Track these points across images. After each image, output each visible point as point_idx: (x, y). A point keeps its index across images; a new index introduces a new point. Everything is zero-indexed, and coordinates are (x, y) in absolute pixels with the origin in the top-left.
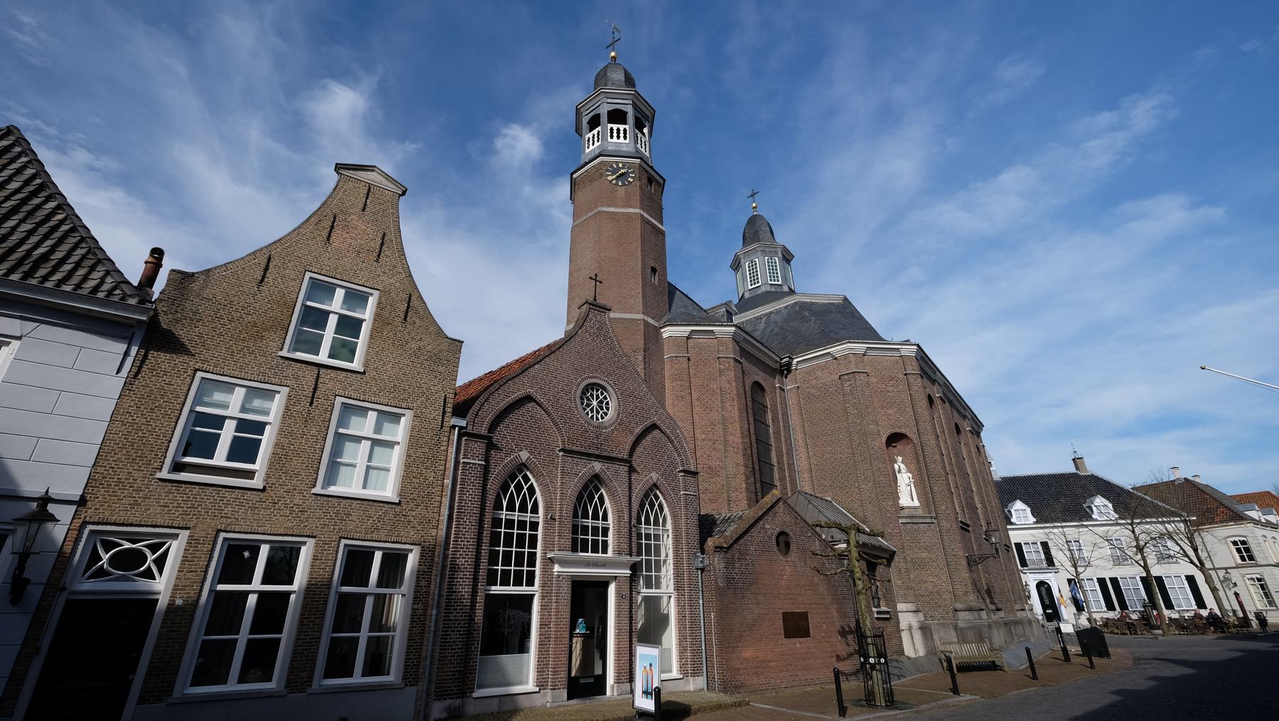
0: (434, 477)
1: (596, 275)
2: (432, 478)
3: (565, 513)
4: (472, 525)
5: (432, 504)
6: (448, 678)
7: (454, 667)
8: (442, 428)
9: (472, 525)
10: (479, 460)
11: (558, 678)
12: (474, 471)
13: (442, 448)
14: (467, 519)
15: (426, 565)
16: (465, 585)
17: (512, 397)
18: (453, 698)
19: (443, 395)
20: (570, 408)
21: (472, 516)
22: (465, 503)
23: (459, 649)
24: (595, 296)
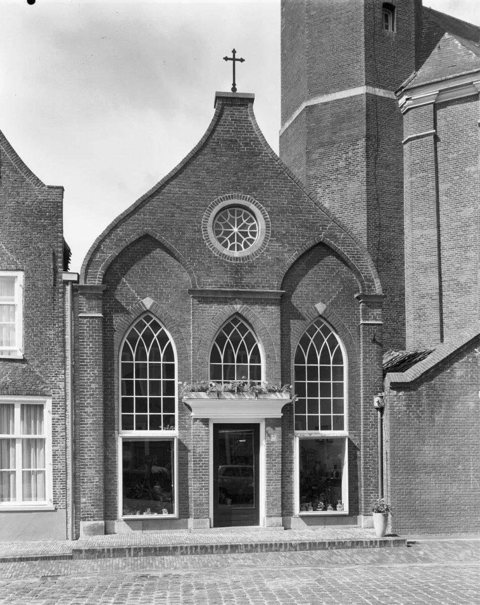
1: (234, 52)
24: (234, 84)
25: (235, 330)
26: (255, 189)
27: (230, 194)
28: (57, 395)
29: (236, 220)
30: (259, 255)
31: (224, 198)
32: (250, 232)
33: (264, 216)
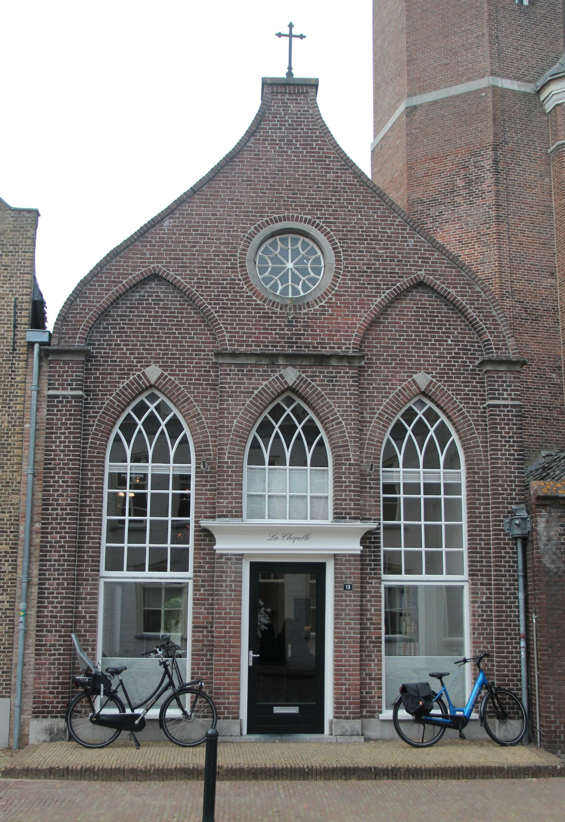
0: (9, 422)
2: (6, 424)
3: (228, 458)
4: (67, 486)
5: (10, 460)
6: (47, 691)
7: (54, 678)
8: (14, 350)
9: (67, 486)
10: (72, 389)
11: (224, 703)
12: (66, 406)
13: (18, 379)
14: (59, 477)
15: (8, 544)
16: (63, 570)
17: (124, 281)
18: (57, 717)
19: (13, 300)
20: (233, 283)
21: (68, 473)
22: (55, 455)
23: (59, 654)
25: (288, 415)
26: (319, 207)
27: (281, 215)
28: (8, 515)
29: (290, 251)
30: (324, 301)
31: (271, 220)
32: (312, 269)
33: (332, 245)
